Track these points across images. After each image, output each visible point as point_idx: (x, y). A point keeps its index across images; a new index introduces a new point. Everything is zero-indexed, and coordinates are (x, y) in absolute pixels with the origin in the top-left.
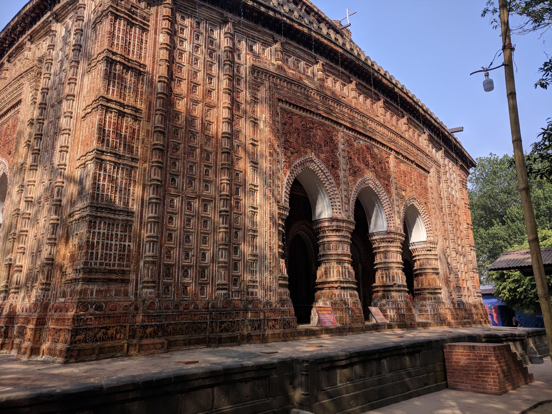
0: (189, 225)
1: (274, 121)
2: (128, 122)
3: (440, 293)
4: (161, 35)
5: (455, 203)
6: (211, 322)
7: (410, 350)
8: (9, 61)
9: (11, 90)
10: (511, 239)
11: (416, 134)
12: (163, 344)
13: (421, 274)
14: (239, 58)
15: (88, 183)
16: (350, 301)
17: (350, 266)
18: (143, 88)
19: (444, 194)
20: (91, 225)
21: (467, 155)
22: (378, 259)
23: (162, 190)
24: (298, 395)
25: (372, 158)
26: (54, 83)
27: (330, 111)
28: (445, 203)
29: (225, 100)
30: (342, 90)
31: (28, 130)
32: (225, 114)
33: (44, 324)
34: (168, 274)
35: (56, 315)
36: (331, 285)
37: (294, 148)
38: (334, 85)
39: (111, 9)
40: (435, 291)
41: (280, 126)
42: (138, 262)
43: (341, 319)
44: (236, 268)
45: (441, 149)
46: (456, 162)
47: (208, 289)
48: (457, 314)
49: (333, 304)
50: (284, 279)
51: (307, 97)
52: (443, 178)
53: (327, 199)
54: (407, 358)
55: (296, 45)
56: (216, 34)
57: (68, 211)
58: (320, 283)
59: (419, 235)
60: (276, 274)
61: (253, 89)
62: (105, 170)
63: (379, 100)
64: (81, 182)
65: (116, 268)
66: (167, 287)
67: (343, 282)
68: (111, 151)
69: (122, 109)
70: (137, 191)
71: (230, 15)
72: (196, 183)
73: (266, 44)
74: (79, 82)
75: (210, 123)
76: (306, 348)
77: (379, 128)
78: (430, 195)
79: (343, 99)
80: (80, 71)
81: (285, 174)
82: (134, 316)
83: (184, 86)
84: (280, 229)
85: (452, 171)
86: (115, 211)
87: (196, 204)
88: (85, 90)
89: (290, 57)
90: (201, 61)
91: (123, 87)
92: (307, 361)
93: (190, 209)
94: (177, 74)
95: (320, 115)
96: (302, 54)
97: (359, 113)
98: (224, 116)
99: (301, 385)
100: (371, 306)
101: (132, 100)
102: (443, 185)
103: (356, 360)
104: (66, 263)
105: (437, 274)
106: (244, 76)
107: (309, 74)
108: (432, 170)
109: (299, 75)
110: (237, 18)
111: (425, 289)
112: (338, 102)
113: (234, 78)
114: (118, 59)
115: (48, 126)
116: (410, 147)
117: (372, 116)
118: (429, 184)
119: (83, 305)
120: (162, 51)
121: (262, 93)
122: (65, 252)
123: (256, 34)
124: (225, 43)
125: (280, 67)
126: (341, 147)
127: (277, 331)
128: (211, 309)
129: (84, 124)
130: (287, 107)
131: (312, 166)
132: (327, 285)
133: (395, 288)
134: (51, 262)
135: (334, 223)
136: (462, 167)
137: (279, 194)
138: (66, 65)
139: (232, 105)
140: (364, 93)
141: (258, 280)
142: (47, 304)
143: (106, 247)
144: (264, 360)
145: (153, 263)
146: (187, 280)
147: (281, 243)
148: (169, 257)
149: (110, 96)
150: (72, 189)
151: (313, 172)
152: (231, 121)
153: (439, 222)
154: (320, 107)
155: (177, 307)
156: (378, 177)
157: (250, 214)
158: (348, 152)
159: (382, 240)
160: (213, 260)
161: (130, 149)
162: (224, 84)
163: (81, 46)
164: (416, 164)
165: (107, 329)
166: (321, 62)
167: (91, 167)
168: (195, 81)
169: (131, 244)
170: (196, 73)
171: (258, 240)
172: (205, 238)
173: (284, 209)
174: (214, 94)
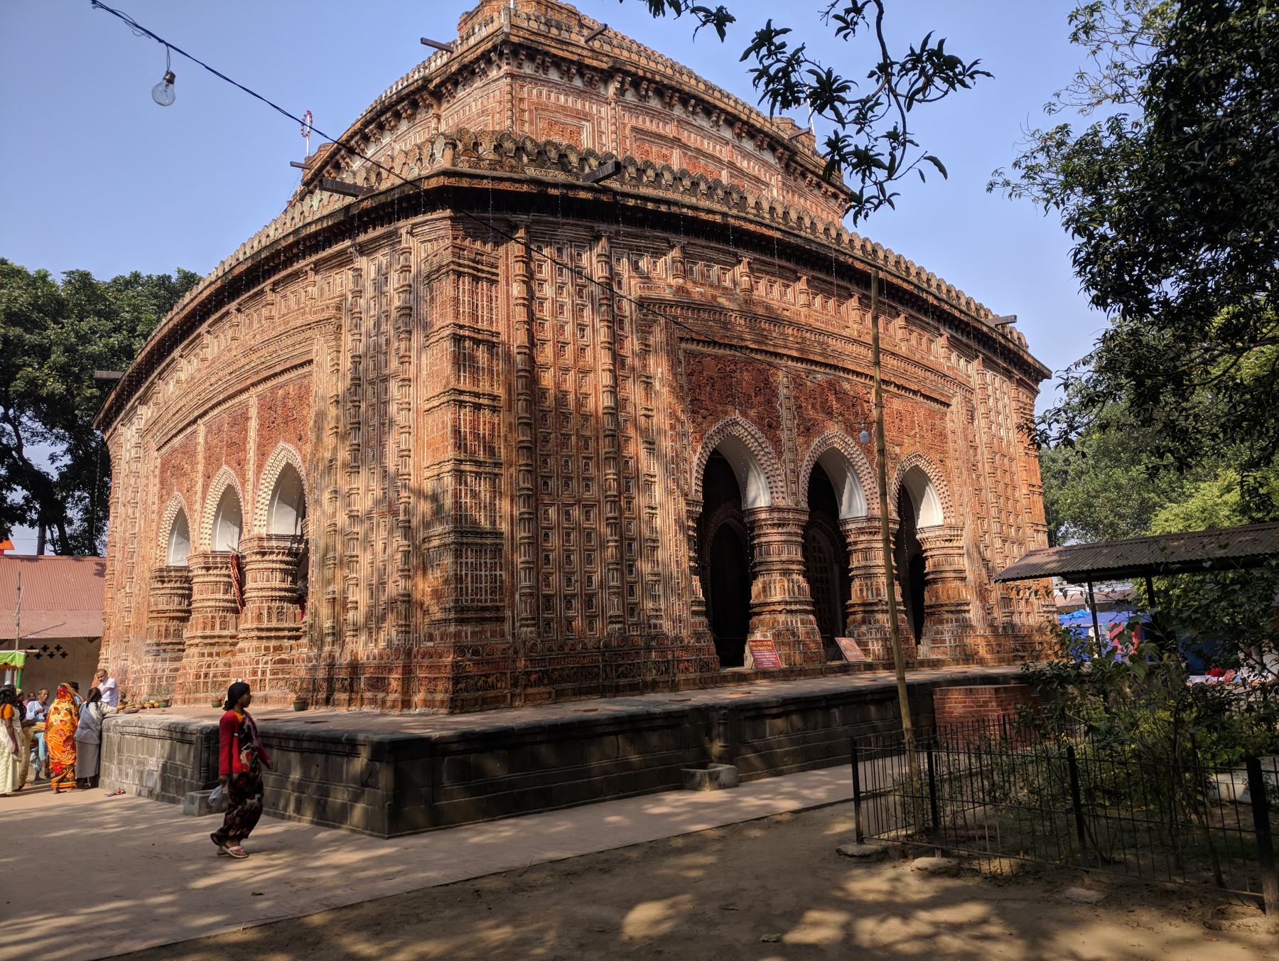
1: (675, 375)
3: (968, 611)
4: (515, 285)
5: (1005, 451)
7: (877, 697)
8: (273, 290)
9: (290, 342)
10: (1174, 491)
11: (924, 340)
12: (550, 693)
13: (935, 581)
14: (620, 288)
15: (448, 502)
16: (801, 630)
17: (801, 578)
18: (500, 366)
19: (982, 439)
20: (458, 555)
21: (1030, 360)
22: (856, 561)
23: (534, 499)
24: (717, 747)
25: (838, 399)
26: (368, 348)
27: (762, 337)
28: (984, 454)
29: (604, 359)
30: (783, 294)
31: (333, 411)
32: (606, 379)
33: (410, 672)
34: (548, 608)
35: (426, 662)
37: (707, 409)
39: (452, 266)
40: (959, 608)
41: (684, 381)
42: (513, 595)
43: (788, 658)
44: (632, 593)
45: (977, 357)
46: (1008, 374)
47: (598, 624)
48: (999, 645)
49: (777, 635)
51: (725, 325)
52: (981, 409)
53: (763, 478)
54: (873, 708)
55: (703, 243)
56: (585, 257)
57: (421, 535)
59: (931, 515)
60: (688, 598)
61: (643, 332)
62: (466, 484)
63: (852, 296)
64: (434, 498)
65: (488, 604)
66: (548, 623)
67: (790, 603)
68: (473, 458)
69: (477, 400)
70: (505, 506)
71: (603, 227)
73: (657, 254)
74: (414, 359)
75: (586, 396)
76: (731, 695)
78: (951, 444)
79: (786, 313)
80: (414, 344)
81: (695, 451)
82: (514, 661)
83: (549, 350)
84: (691, 533)
85: (999, 392)
86: (482, 534)
87: (576, 513)
88: (424, 373)
89: (695, 263)
91: (475, 370)
93: (568, 520)
94: (539, 336)
95: (747, 348)
96: (714, 255)
97: (812, 330)
98: (605, 383)
99: (719, 736)
101: (487, 384)
102: (980, 422)
103: (792, 708)
104: (428, 600)
105: (963, 579)
106: (627, 313)
107: (728, 284)
109: (710, 291)
110: (614, 228)
112: (775, 319)
113: (615, 322)
114: (467, 333)
116: (909, 368)
117: (836, 331)
118: (949, 426)
119: (460, 650)
120: (517, 309)
121: (658, 336)
122: (424, 587)
123: (643, 243)
124: (599, 272)
125: (680, 289)
126: (783, 391)
127: (691, 676)
128: (606, 648)
129: (430, 419)
131: (738, 431)
132: (767, 609)
133: (880, 607)
134: (407, 598)
135: (776, 515)
136: (1020, 383)
139: (614, 364)
140: (822, 291)
141: (663, 607)
142: (411, 649)
143: (476, 579)
144: (675, 707)
145: (531, 594)
146: (571, 613)
147: (692, 554)
148: (548, 585)
149: (462, 387)
150: (425, 507)
151: (738, 440)
152: (613, 390)
153: (968, 491)
154: (747, 336)
155: (561, 648)
157: (645, 517)
158: (795, 397)
159: (861, 531)
160: (601, 585)
161: (491, 451)
162: (603, 335)
163: (411, 308)
164: (922, 395)
165: (487, 676)
166: (746, 260)
167: (448, 480)
168: (561, 339)
169: (503, 573)
170: (562, 327)
171: (660, 554)
172: (589, 556)
173: (696, 503)
174: (589, 352)
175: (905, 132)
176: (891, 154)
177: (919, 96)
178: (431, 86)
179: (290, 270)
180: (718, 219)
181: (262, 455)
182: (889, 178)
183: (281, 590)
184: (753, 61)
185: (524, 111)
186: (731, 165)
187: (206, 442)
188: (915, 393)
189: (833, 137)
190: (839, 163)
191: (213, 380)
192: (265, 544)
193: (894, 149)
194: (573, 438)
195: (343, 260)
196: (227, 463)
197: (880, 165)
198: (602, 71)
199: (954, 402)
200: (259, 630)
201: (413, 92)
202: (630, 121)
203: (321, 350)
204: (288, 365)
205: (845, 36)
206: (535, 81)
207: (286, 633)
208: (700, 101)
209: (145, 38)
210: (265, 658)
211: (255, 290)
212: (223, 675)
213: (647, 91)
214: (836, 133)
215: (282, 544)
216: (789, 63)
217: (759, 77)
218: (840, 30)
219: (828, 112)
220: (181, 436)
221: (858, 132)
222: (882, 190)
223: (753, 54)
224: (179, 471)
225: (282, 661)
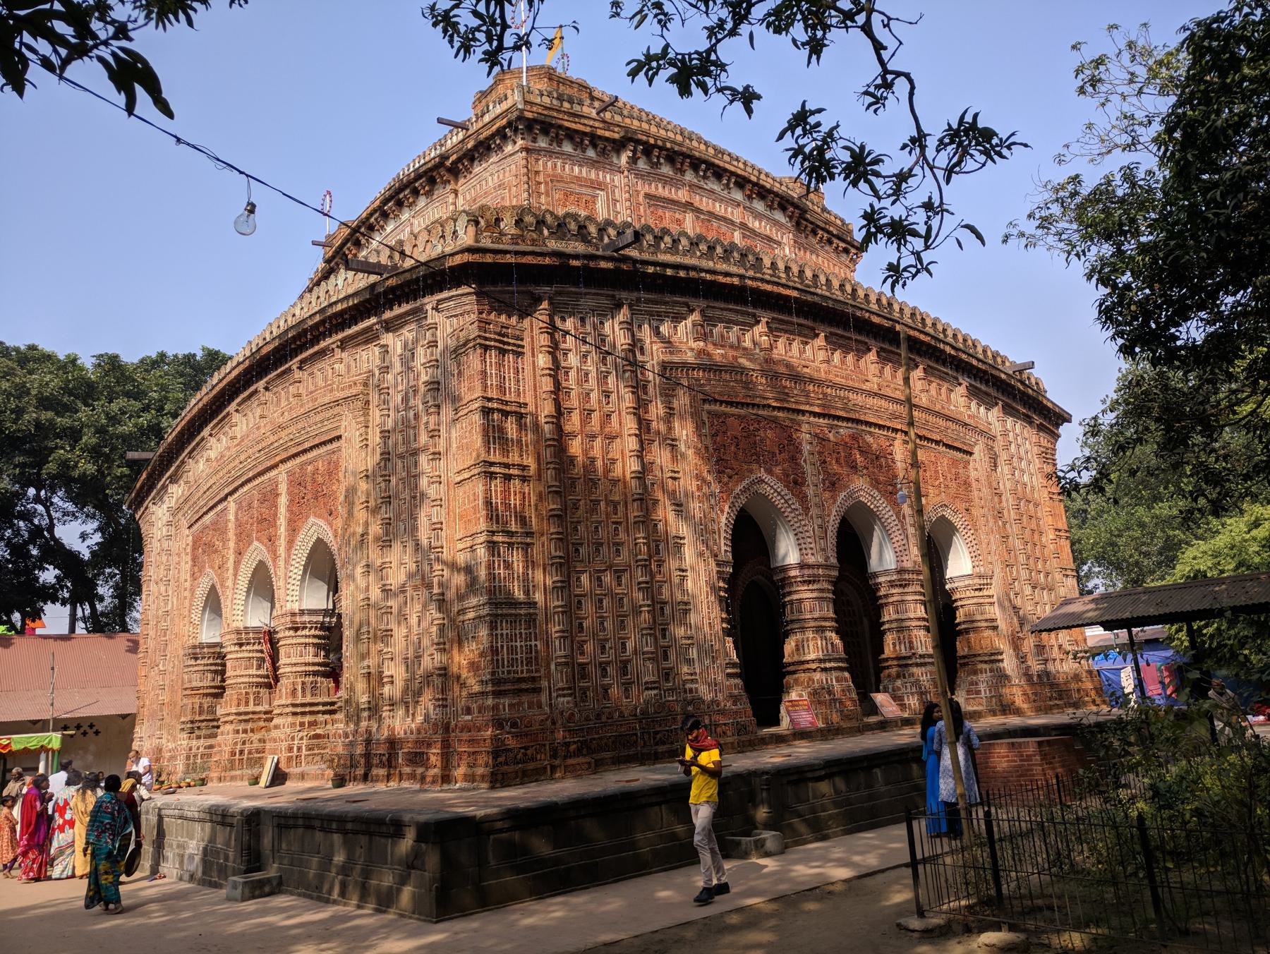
0: (601, 608)
1: (700, 436)
2: (516, 484)
3: (1002, 661)
4: (540, 356)
6: (642, 733)
8: (300, 368)
9: (318, 418)
11: (944, 390)
13: (967, 631)
14: (643, 353)
15: (483, 573)
16: (837, 687)
17: (834, 635)
18: (529, 437)
19: (1006, 486)
20: (493, 627)
21: (1049, 405)
22: (888, 615)
23: (566, 566)
24: (762, 813)
25: (861, 452)
26: (396, 424)
27: (784, 395)
28: (1008, 501)
29: (630, 424)
30: (802, 352)
31: (363, 486)
32: (632, 444)
34: (584, 676)
35: (465, 736)
36: (807, 666)
38: (790, 351)
40: (993, 658)
41: (709, 442)
44: (666, 658)
45: (997, 404)
46: (1028, 420)
47: (634, 690)
49: (814, 693)
50: (734, 665)
51: (748, 385)
52: (1004, 456)
56: (607, 325)
58: (790, 664)
59: (959, 565)
61: (667, 395)
62: (499, 555)
63: (870, 350)
64: (468, 570)
65: (525, 675)
66: (584, 691)
68: (504, 529)
69: (507, 471)
71: (624, 295)
72: (604, 550)
73: (678, 318)
74: (443, 432)
75: (613, 461)
76: (772, 758)
77: (871, 402)
78: (976, 493)
79: (805, 370)
81: (722, 511)
83: (576, 418)
84: (722, 594)
86: (515, 604)
87: (608, 578)
89: (715, 326)
90: (593, 375)
92: (767, 773)
93: (600, 586)
94: (566, 404)
95: (769, 406)
96: (733, 316)
97: (833, 386)
99: (762, 802)
100: (878, 691)
102: (1003, 469)
103: (835, 770)
105: (995, 628)
108: (978, 450)
109: (731, 353)
111: (975, 656)
112: (797, 378)
113: (639, 387)
114: (495, 405)
115: (397, 485)
116: (930, 418)
117: (856, 385)
118: (973, 474)
119: (498, 723)
120: (544, 379)
121: (682, 400)
123: (663, 308)
125: (701, 352)
126: (806, 448)
127: (730, 740)
129: (460, 491)
130: (716, 407)
132: (802, 667)
133: (914, 661)
134: (444, 672)
135: (806, 572)
136: (1041, 428)
137: (715, 544)
138: (417, 402)
139: (639, 429)
140: (840, 346)
142: (448, 723)
143: (512, 650)
145: (566, 664)
146: (607, 681)
147: (724, 616)
148: (582, 653)
150: (459, 580)
153: (995, 539)
155: (598, 716)
156: (875, 483)
157: (676, 580)
158: (819, 453)
159: (892, 584)
161: (523, 520)
162: (628, 400)
163: (438, 383)
165: (526, 748)
167: (482, 552)
169: (538, 643)
170: (588, 394)
171: (693, 618)
172: (622, 621)
173: (725, 563)
174: (614, 418)
175: (942, 203)
176: (926, 223)
177: (957, 169)
178: (448, 163)
179: (316, 348)
180: (736, 281)
181: (293, 530)
182: (927, 247)
183: (314, 664)
184: (789, 141)
185: (540, 183)
186: (743, 226)
187: (237, 519)
188: (937, 442)
189: (869, 210)
190: (875, 235)
191: (242, 457)
192: (298, 619)
193: (929, 217)
194: (603, 504)
195: (369, 337)
196: (258, 539)
197: (915, 234)
198: (614, 141)
199: (976, 450)
200: (294, 705)
201: (431, 170)
202: (643, 188)
203: (349, 425)
204: (317, 441)
205: (875, 111)
206: (550, 153)
207: (320, 708)
208: (710, 165)
209: (227, 171)
210: (301, 734)
211: (283, 368)
212: (258, 751)
213: (658, 158)
214: (871, 205)
215: (314, 619)
216: (824, 140)
217: (795, 156)
218: (870, 105)
219: (862, 185)
220: (212, 513)
221: (893, 203)
222: (919, 259)
223: (789, 133)
224: (210, 549)
225: (317, 736)
